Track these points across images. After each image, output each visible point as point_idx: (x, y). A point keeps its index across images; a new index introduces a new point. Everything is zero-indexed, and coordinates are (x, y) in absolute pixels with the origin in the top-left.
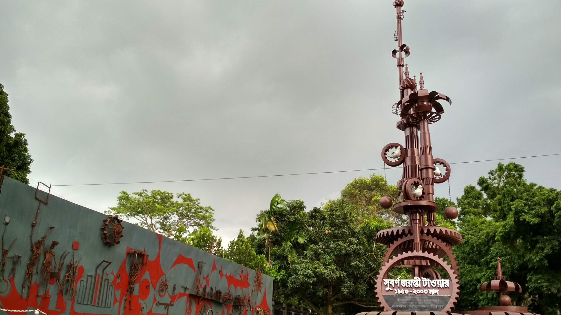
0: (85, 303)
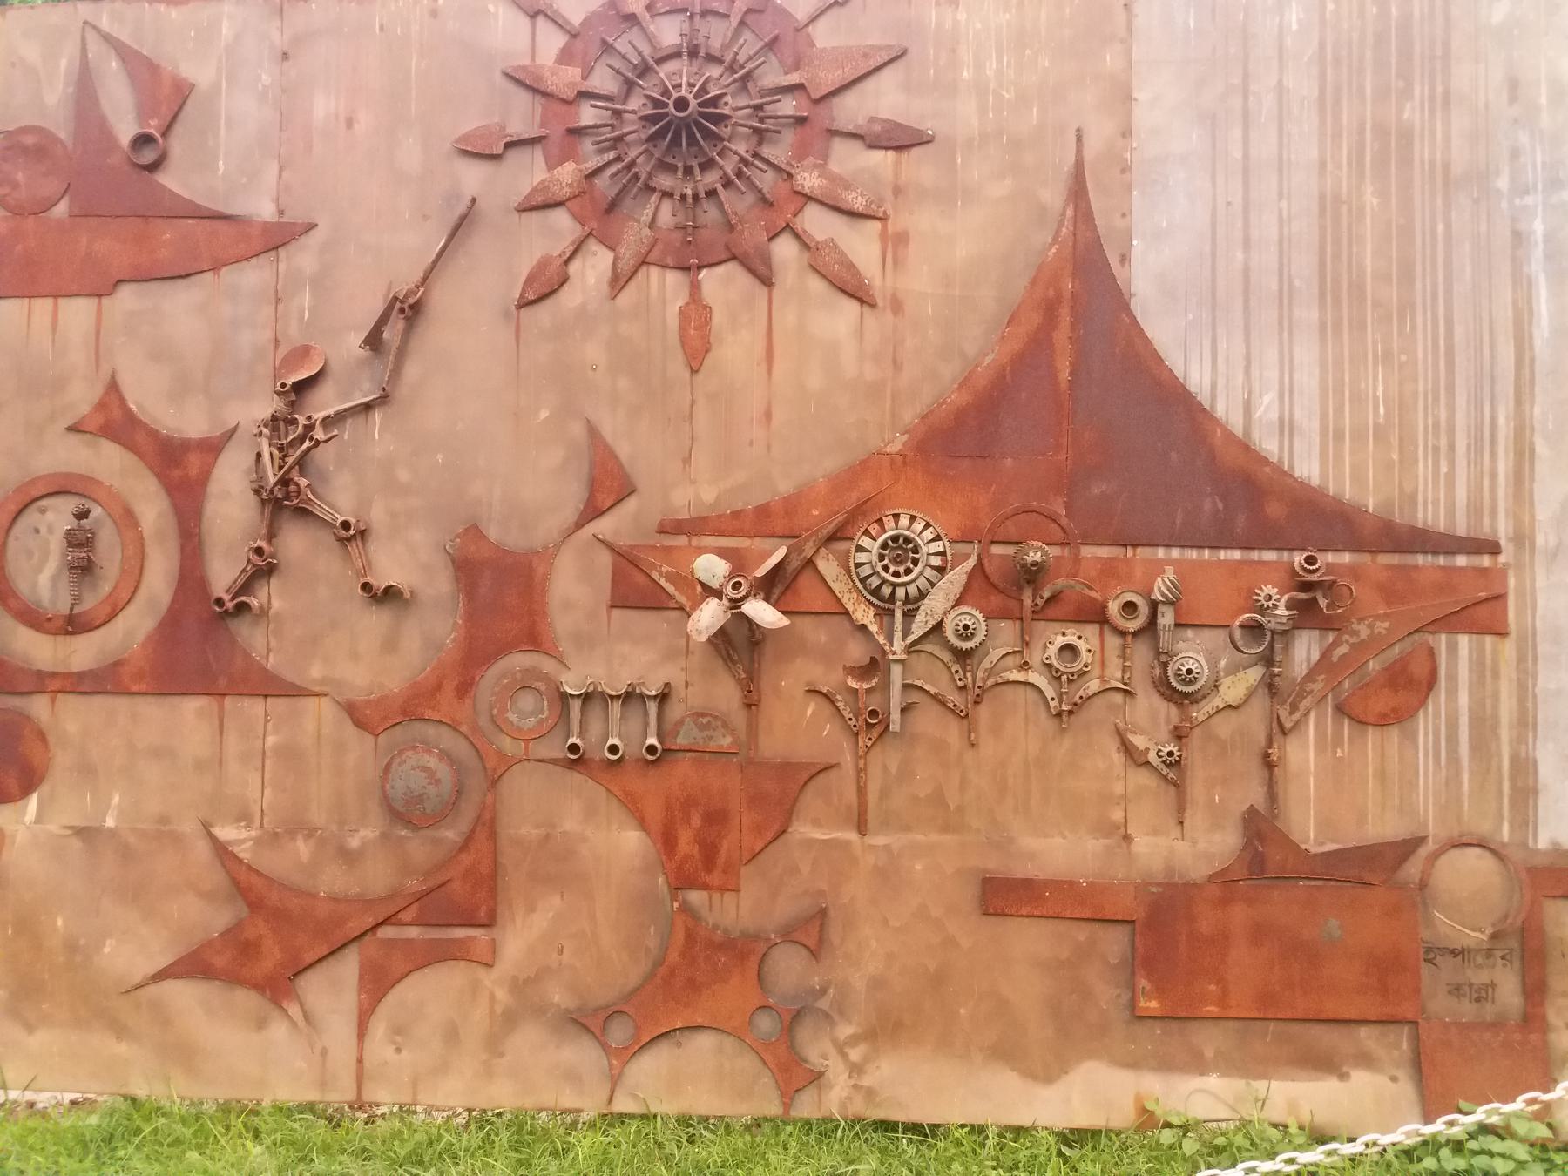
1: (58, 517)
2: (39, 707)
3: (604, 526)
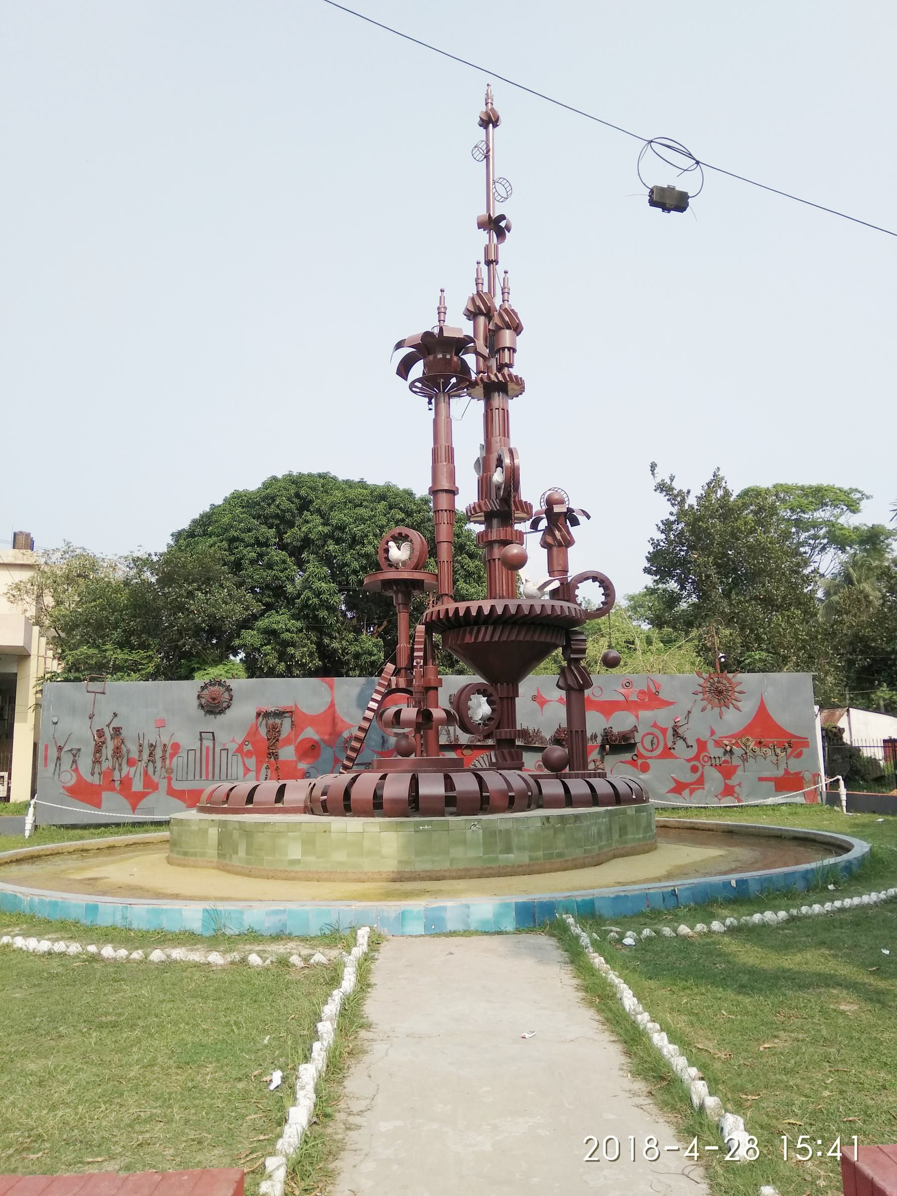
0: (191, 777)
1: (651, 737)
2: (648, 761)
3: (713, 738)
